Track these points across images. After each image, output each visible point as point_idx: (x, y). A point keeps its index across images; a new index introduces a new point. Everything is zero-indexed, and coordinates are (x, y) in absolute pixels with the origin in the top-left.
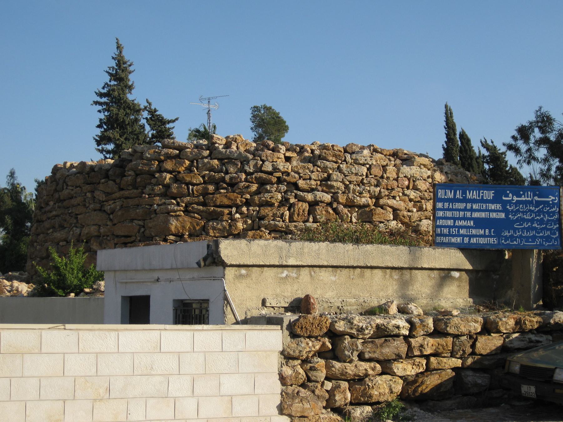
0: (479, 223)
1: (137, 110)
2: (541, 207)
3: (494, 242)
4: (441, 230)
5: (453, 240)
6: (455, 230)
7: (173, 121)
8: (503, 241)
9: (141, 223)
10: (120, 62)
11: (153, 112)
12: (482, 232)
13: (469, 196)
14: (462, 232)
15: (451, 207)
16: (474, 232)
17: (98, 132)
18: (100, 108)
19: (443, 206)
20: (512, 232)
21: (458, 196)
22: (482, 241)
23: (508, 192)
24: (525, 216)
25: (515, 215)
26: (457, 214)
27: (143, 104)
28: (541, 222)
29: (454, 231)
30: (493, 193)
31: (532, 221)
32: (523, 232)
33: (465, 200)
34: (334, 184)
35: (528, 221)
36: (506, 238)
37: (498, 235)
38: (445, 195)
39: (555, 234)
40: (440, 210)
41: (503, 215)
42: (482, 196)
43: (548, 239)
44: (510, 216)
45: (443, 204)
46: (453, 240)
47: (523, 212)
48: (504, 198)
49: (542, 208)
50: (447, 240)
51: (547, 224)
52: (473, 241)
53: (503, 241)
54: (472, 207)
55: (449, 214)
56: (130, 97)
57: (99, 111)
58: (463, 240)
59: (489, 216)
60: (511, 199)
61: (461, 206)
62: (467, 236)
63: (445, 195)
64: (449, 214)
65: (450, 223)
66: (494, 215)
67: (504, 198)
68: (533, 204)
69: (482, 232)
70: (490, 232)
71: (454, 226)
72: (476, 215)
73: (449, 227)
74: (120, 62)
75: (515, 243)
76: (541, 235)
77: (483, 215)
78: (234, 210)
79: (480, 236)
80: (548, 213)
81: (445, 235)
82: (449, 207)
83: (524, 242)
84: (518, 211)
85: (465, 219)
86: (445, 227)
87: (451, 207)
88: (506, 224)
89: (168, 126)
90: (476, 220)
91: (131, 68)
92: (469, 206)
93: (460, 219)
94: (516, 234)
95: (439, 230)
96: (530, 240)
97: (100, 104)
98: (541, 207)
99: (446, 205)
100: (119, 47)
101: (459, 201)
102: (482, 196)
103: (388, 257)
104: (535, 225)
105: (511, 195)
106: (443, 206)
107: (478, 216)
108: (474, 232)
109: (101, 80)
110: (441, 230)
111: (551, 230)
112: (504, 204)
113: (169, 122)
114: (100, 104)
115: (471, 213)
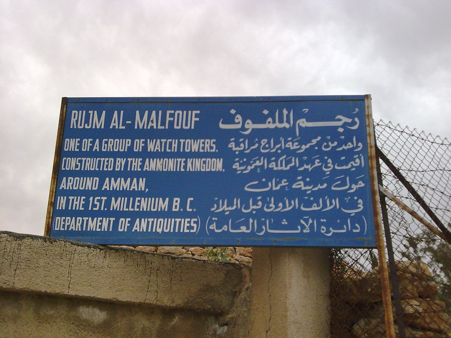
0: (160, 184)
2: (314, 141)
3: (190, 228)
4: (68, 201)
5: (93, 224)
6: (100, 201)
8: (213, 227)
12: (163, 205)
14: (115, 204)
15: (96, 147)
16: (144, 204)
19: (80, 147)
20: (237, 203)
21: (117, 122)
22: (162, 226)
23: (233, 111)
24: (273, 165)
25: (247, 164)
26: (108, 164)
28: (316, 177)
29: (98, 203)
30: (196, 116)
31: (292, 175)
32: (266, 203)
33: (131, 132)
35: (280, 175)
36: (222, 219)
37: (202, 212)
38: (87, 122)
39: (354, 205)
40: (72, 154)
41: (218, 165)
42: (171, 123)
44: (236, 166)
45: (80, 142)
46: (93, 224)
47: (268, 156)
48: (222, 126)
49: (319, 144)
50: (79, 225)
51: (330, 181)
52: (141, 225)
53: (213, 227)
54: (145, 148)
55: (90, 164)
58: (116, 223)
59: (185, 167)
60: (239, 126)
61: (121, 145)
62: (125, 214)
63: (87, 122)
64: (90, 164)
65: (90, 183)
66: (196, 165)
67: (222, 126)
68: (294, 136)
69: (163, 205)
70: (183, 204)
71: (100, 192)
72: (153, 165)
73: (87, 193)
75: (243, 229)
76: (315, 208)
77: (171, 165)
81: (75, 214)
82: (92, 148)
83: (266, 229)
84: (256, 153)
85: (126, 174)
87: (96, 147)
88: (227, 184)
90: (152, 177)
92: (139, 145)
93: (115, 175)
94: (247, 207)
95: (62, 202)
96: (285, 222)
98: (314, 141)
99: (87, 143)
102: (171, 123)
104: (299, 185)
105: (239, 118)
106: (80, 147)
107: (159, 167)
108: (144, 204)
110: (68, 201)
111: (342, 195)
112: (223, 138)
115: (143, 162)
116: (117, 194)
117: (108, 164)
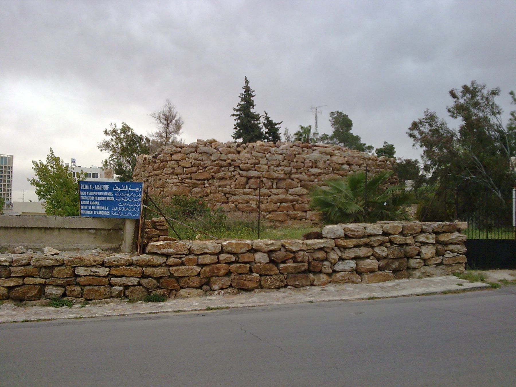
0: (102, 203)
1: (257, 117)
5: (89, 212)
7: (279, 124)
9: (162, 189)
10: (247, 89)
11: (267, 119)
13: (96, 188)
14: (93, 208)
16: (99, 208)
17: (235, 131)
18: (235, 118)
22: (103, 213)
26: (91, 198)
27: (262, 114)
28: (131, 203)
29: (89, 207)
31: (127, 202)
33: (94, 190)
34: (262, 166)
35: (125, 202)
36: (114, 212)
37: (110, 210)
40: (82, 195)
41: (113, 199)
43: (134, 212)
46: (89, 212)
52: (99, 213)
55: (87, 198)
56: (252, 110)
57: (235, 120)
61: (92, 193)
64: (87, 198)
65: (87, 203)
66: (109, 199)
71: (89, 205)
72: (100, 198)
73: (87, 205)
74: (247, 89)
77: (103, 199)
78: (206, 182)
79: (102, 210)
80: (135, 198)
85: (94, 201)
86: (85, 205)
89: (276, 127)
90: (101, 202)
91: (253, 94)
97: (236, 115)
100: (247, 82)
101: (92, 191)
103: (40, 222)
104: (129, 205)
105: (117, 187)
108: (99, 208)
109: (236, 101)
113: (276, 124)
114: (236, 115)
116: (92, 205)
117: (91, 198)
